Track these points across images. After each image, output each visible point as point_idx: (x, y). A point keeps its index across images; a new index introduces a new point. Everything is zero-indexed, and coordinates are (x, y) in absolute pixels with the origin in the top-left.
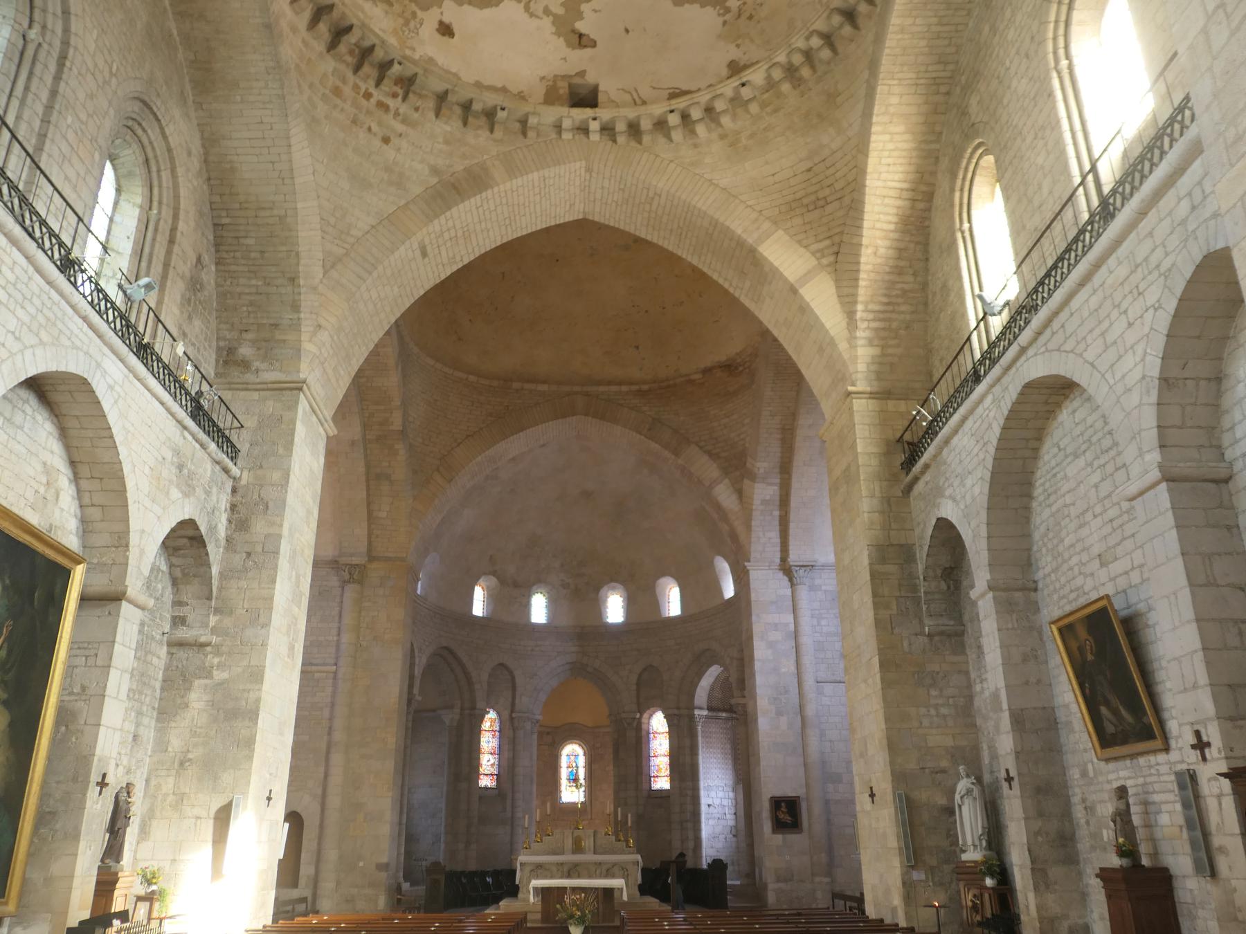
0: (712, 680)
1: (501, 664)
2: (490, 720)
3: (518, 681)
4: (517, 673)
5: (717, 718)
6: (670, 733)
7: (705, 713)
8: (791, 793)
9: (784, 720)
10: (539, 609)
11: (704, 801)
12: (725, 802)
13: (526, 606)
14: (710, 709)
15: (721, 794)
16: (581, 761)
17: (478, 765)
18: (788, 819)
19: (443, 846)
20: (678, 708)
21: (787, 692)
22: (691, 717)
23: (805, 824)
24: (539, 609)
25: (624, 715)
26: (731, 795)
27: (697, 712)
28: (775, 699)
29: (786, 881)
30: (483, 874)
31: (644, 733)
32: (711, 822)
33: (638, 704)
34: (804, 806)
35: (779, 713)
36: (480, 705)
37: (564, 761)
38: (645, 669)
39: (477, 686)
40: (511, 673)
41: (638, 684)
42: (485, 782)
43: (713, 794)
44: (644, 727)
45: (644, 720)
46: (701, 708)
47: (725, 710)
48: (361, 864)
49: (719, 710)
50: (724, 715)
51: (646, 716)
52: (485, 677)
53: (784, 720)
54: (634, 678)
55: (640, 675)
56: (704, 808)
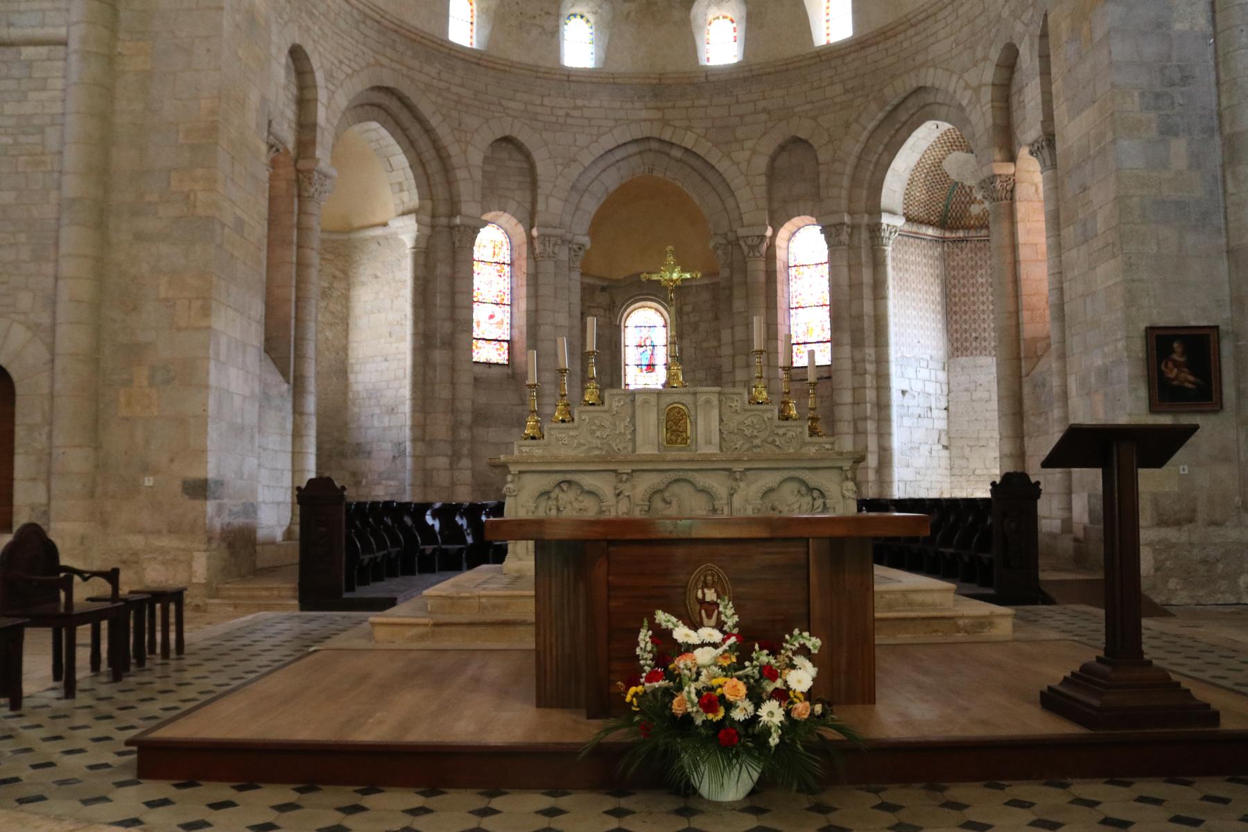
0: (915, 157)
1: (507, 140)
2: (493, 245)
3: (540, 169)
4: (539, 156)
5: (916, 236)
6: (832, 261)
7: (900, 222)
8: (1193, 319)
9: (1179, 147)
10: (579, 46)
11: (897, 383)
12: (931, 388)
13: (554, 35)
14: (909, 219)
15: (924, 373)
16: (660, 336)
17: (468, 324)
18: (1188, 379)
19: (409, 461)
20: (851, 213)
21: (1186, 79)
22: (875, 230)
23: (1229, 392)
24: (579, 46)
25: (741, 232)
26: (942, 376)
27: (886, 219)
28: (1158, 96)
29: (1178, 523)
30: (422, 508)
31: (779, 265)
32: (907, 422)
33: (772, 213)
34: (1227, 348)
35: (1168, 131)
36: (469, 208)
37: (631, 336)
38: (782, 148)
39: (461, 174)
40: (527, 156)
41: (772, 174)
42: (488, 353)
43: (910, 372)
44: (780, 254)
45: (780, 241)
46: (893, 213)
47: (929, 223)
48: (149, 481)
49: (921, 222)
50: (930, 231)
51: (783, 233)
52: (476, 157)
53: (1179, 147)
54: (762, 163)
55: (773, 159)
56: (895, 396)
